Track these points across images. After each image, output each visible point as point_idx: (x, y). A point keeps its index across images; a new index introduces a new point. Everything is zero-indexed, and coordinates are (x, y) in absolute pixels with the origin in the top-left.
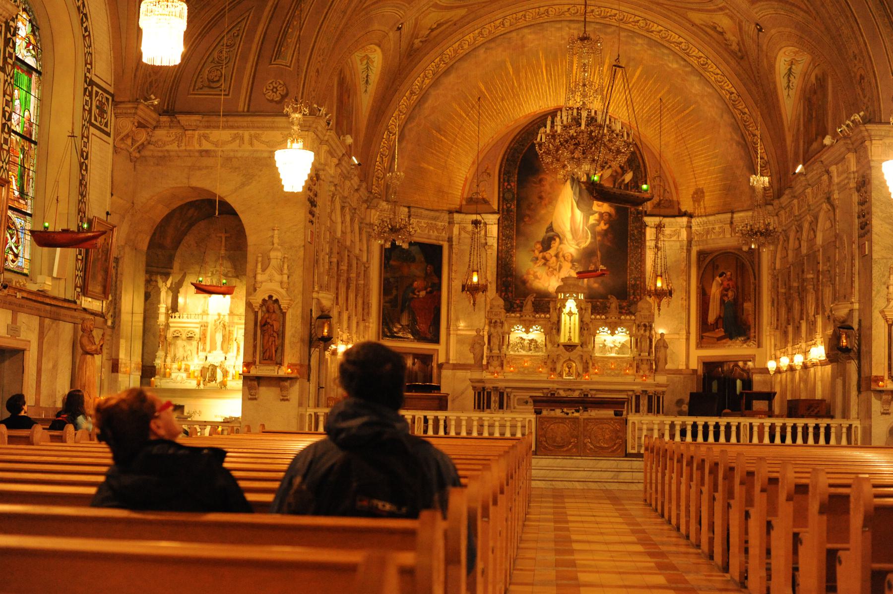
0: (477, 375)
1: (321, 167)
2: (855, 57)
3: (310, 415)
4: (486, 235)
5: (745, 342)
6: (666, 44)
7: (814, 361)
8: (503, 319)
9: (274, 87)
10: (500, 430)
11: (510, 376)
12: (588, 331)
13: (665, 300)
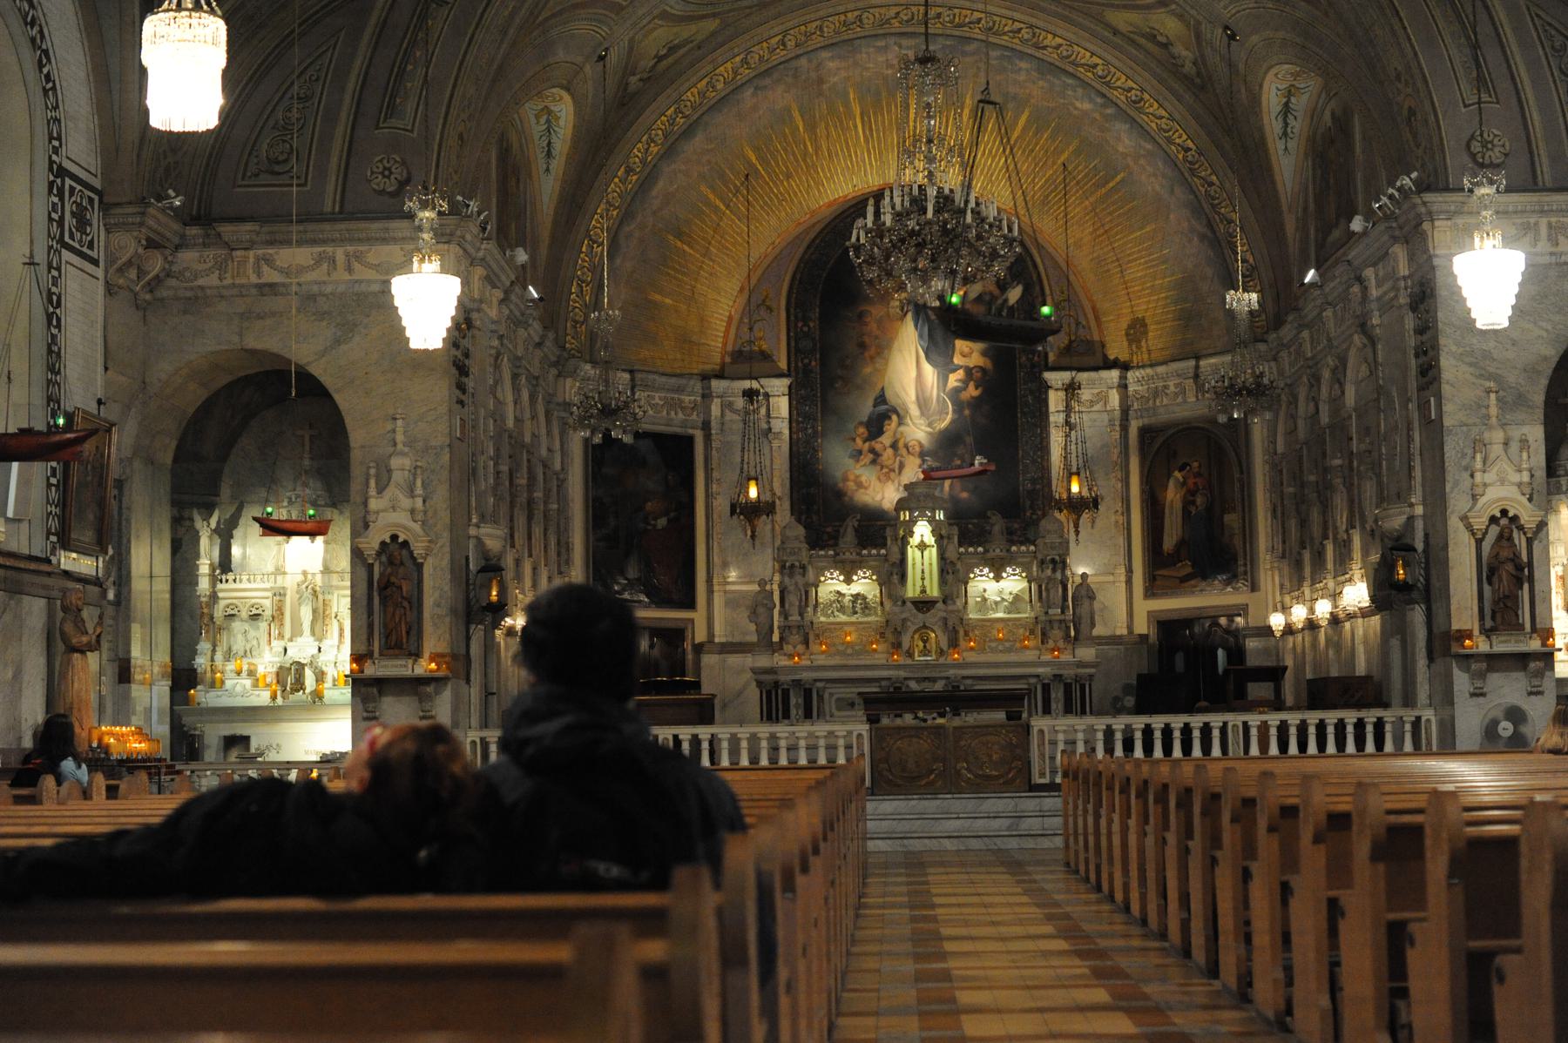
0: (763, 661)
1: (475, 305)
2: (1398, 77)
3: (474, 742)
4: (768, 415)
5: (1228, 583)
7: (1351, 609)
8: (805, 562)
9: (385, 168)
10: (807, 755)
11: (821, 660)
12: (952, 573)
13: (1085, 516)
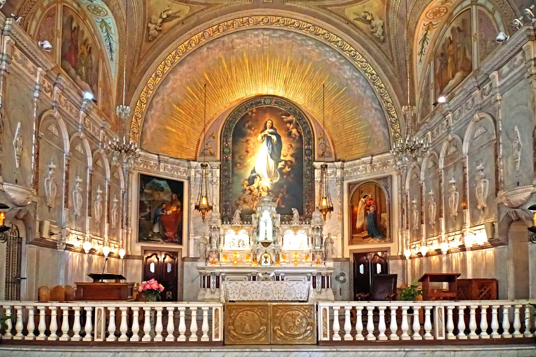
6: (328, 44)
8: (219, 226)
